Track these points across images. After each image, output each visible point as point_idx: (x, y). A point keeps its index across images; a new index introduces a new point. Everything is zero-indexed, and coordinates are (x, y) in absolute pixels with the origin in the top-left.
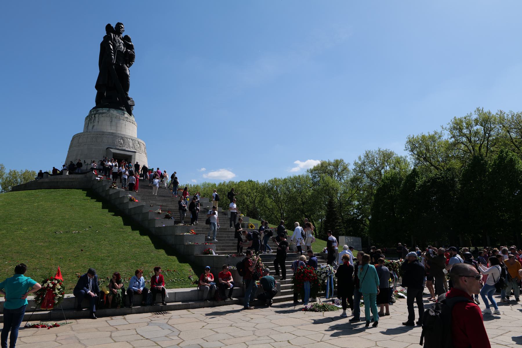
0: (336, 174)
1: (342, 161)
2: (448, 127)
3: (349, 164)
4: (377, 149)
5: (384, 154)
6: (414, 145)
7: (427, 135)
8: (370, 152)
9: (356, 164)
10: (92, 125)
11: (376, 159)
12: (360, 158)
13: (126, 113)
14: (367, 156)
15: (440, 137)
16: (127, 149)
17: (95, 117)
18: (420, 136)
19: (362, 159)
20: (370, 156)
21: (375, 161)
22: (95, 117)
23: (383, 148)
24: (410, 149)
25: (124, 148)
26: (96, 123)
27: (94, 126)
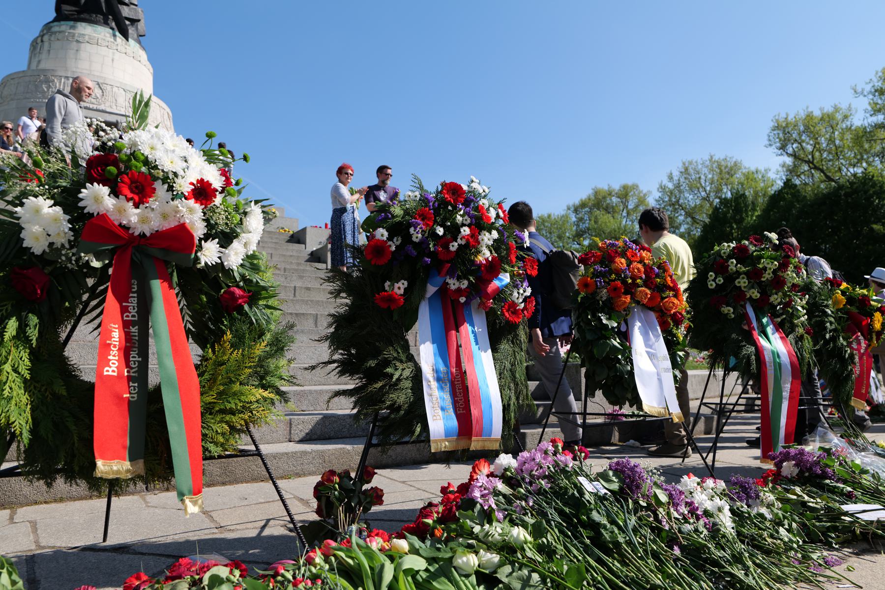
0: (624, 214)
1: (635, 187)
2: (868, 88)
3: (650, 192)
4: (707, 157)
5: (719, 166)
6: (784, 135)
7: (817, 113)
8: (691, 163)
9: (662, 188)
10: (37, 59)
11: (703, 177)
12: (671, 178)
13: (117, 34)
14: (686, 171)
15: (846, 117)
16: (108, 110)
17: (42, 41)
18: (802, 115)
19: (676, 178)
20: (691, 171)
21: (702, 181)
22: (42, 41)
23: (719, 156)
24: (778, 145)
25: (102, 107)
26: (44, 56)
27: (39, 62)
